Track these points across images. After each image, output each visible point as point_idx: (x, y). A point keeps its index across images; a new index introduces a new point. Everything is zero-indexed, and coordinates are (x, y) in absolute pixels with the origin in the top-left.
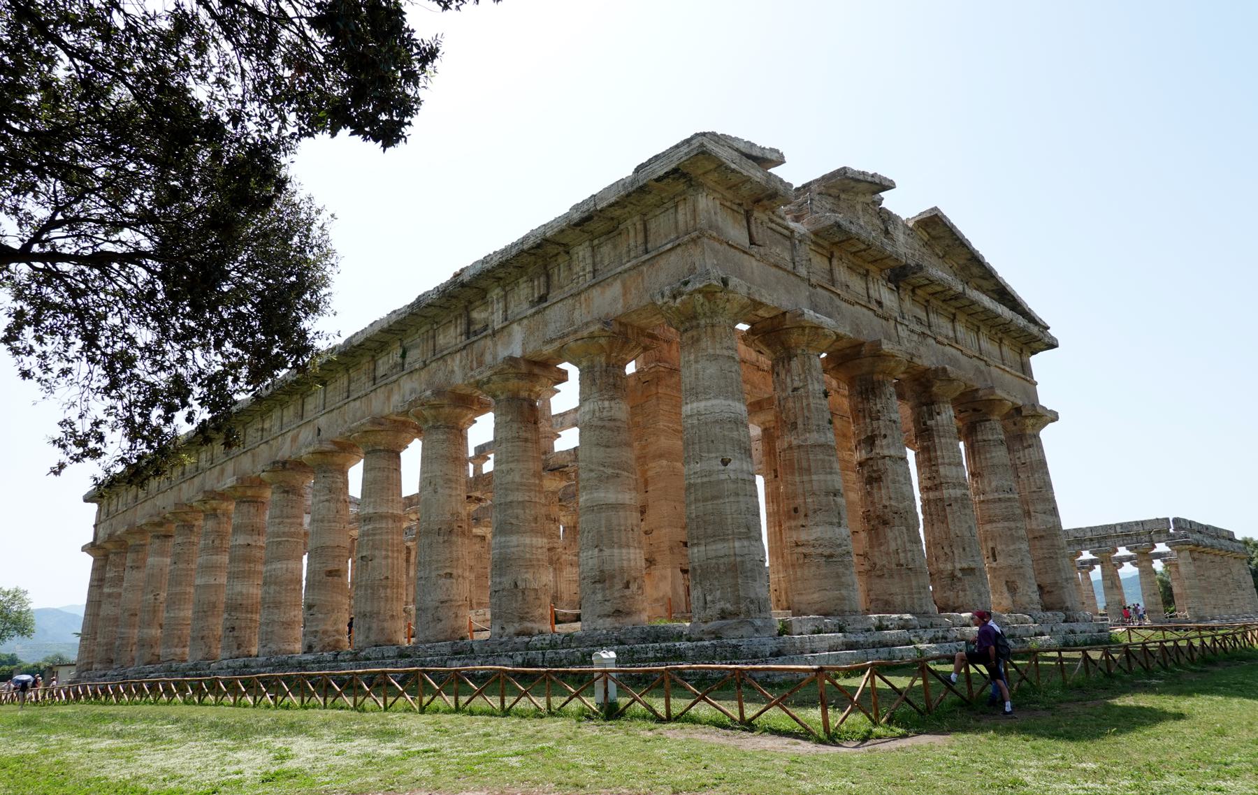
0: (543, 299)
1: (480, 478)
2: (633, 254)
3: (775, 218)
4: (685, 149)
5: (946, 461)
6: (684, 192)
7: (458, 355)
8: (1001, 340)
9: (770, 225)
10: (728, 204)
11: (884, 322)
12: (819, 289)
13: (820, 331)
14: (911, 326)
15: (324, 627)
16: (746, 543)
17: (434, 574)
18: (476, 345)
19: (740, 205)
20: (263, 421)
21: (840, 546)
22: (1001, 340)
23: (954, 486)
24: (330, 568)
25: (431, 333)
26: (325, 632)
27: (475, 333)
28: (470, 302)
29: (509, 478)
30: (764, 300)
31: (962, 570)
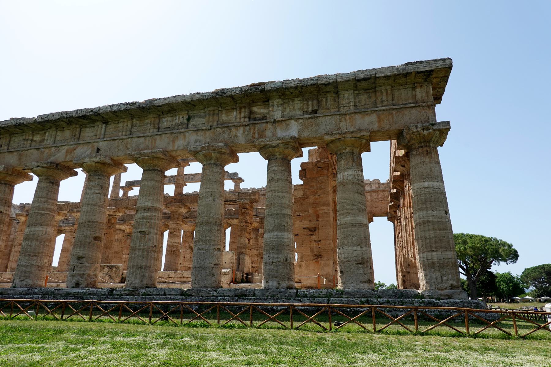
0: (315, 112)
1: (180, 198)
2: (385, 103)
4: (441, 63)
6: (421, 83)
7: (242, 128)
15: (89, 272)
17: (212, 248)
18: (258, 125)
20: (33, 135)
24: (97, 235)
25: (216, 112)
26: (89, 275)
27: (255, 119)
28: (253, 102)
29: (283, 201)
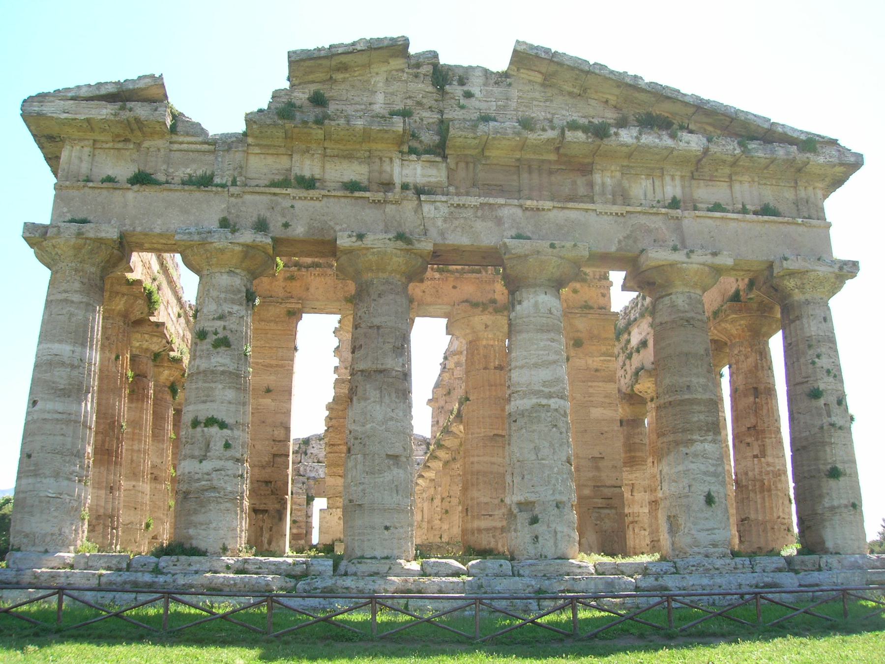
3: (181, 139)
5: (518, 364)
8: (730, 177)
9: (176, 147)
10: (110, 145)
11: (390, 209)
12: (248, 197)
13: (208, 247)
14: (456, 200)
16: (31, 480)
19: (126, 140)
21: (199, 480)
22: (730, 177)
23: (525, 395)
30: (103, 235)
31: (519, 504)
